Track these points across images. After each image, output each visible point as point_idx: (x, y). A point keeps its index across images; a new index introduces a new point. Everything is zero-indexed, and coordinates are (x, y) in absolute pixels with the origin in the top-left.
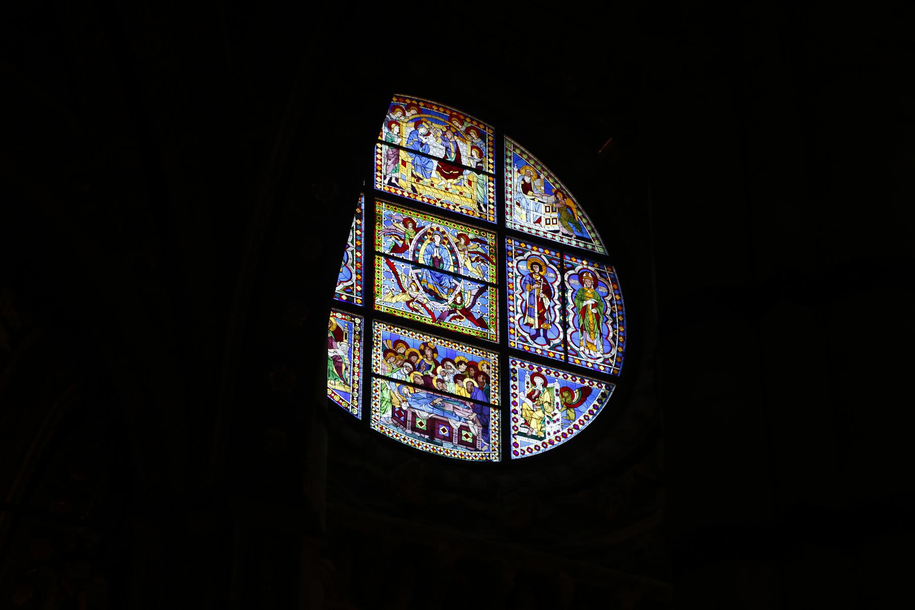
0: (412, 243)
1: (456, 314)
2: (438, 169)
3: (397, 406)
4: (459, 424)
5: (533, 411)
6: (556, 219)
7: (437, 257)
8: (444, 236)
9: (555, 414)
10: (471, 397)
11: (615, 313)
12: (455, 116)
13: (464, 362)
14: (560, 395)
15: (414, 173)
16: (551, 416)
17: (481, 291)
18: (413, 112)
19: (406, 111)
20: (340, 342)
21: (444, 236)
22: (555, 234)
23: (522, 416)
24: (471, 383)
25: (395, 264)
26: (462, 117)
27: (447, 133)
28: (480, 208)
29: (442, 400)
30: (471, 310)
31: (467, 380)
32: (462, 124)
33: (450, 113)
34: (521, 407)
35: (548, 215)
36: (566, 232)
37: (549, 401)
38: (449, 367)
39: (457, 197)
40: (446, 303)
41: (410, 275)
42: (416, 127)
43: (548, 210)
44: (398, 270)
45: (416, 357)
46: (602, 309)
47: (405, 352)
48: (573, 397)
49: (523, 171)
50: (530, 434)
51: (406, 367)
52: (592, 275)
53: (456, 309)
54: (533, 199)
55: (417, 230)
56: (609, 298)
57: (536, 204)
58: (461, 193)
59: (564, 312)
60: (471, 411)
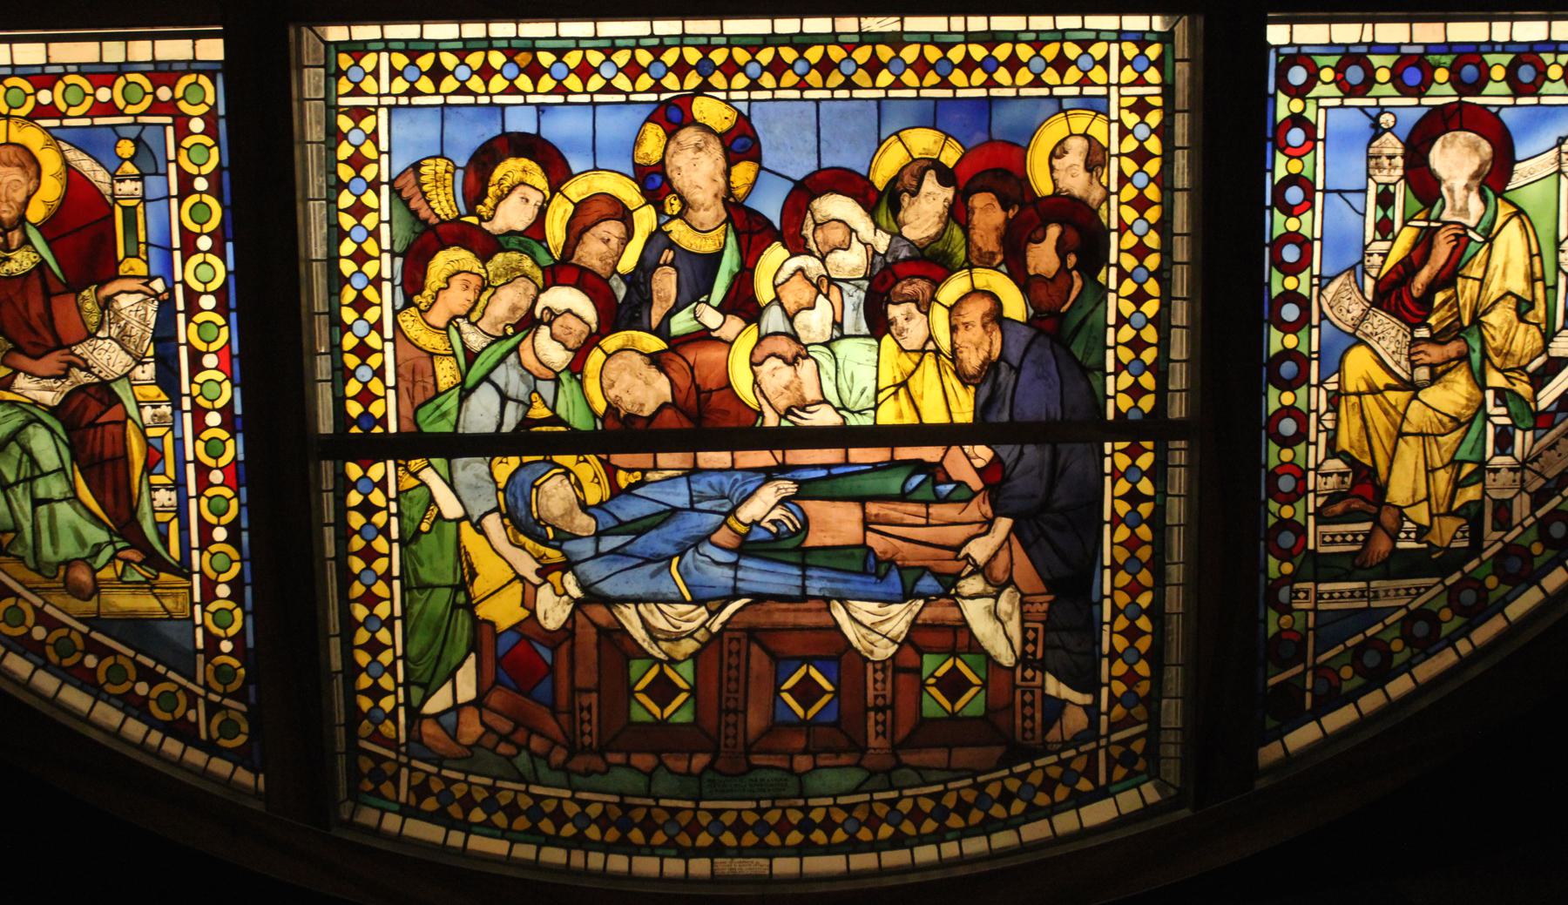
3: (503, 611)
4: (899, 618)
10: (981, 410)
13: (936, 165)
16: (1523, 389)
20: (102, 284)
23: (1332, 450)
24: (985, 305)
29: (789, 488)
37: (1518, 285)
38: (837, 235)
45: (613, 229)
47: (542, 212)
50: (1382, 545)
51: (553, 315)
60: (978, 509)
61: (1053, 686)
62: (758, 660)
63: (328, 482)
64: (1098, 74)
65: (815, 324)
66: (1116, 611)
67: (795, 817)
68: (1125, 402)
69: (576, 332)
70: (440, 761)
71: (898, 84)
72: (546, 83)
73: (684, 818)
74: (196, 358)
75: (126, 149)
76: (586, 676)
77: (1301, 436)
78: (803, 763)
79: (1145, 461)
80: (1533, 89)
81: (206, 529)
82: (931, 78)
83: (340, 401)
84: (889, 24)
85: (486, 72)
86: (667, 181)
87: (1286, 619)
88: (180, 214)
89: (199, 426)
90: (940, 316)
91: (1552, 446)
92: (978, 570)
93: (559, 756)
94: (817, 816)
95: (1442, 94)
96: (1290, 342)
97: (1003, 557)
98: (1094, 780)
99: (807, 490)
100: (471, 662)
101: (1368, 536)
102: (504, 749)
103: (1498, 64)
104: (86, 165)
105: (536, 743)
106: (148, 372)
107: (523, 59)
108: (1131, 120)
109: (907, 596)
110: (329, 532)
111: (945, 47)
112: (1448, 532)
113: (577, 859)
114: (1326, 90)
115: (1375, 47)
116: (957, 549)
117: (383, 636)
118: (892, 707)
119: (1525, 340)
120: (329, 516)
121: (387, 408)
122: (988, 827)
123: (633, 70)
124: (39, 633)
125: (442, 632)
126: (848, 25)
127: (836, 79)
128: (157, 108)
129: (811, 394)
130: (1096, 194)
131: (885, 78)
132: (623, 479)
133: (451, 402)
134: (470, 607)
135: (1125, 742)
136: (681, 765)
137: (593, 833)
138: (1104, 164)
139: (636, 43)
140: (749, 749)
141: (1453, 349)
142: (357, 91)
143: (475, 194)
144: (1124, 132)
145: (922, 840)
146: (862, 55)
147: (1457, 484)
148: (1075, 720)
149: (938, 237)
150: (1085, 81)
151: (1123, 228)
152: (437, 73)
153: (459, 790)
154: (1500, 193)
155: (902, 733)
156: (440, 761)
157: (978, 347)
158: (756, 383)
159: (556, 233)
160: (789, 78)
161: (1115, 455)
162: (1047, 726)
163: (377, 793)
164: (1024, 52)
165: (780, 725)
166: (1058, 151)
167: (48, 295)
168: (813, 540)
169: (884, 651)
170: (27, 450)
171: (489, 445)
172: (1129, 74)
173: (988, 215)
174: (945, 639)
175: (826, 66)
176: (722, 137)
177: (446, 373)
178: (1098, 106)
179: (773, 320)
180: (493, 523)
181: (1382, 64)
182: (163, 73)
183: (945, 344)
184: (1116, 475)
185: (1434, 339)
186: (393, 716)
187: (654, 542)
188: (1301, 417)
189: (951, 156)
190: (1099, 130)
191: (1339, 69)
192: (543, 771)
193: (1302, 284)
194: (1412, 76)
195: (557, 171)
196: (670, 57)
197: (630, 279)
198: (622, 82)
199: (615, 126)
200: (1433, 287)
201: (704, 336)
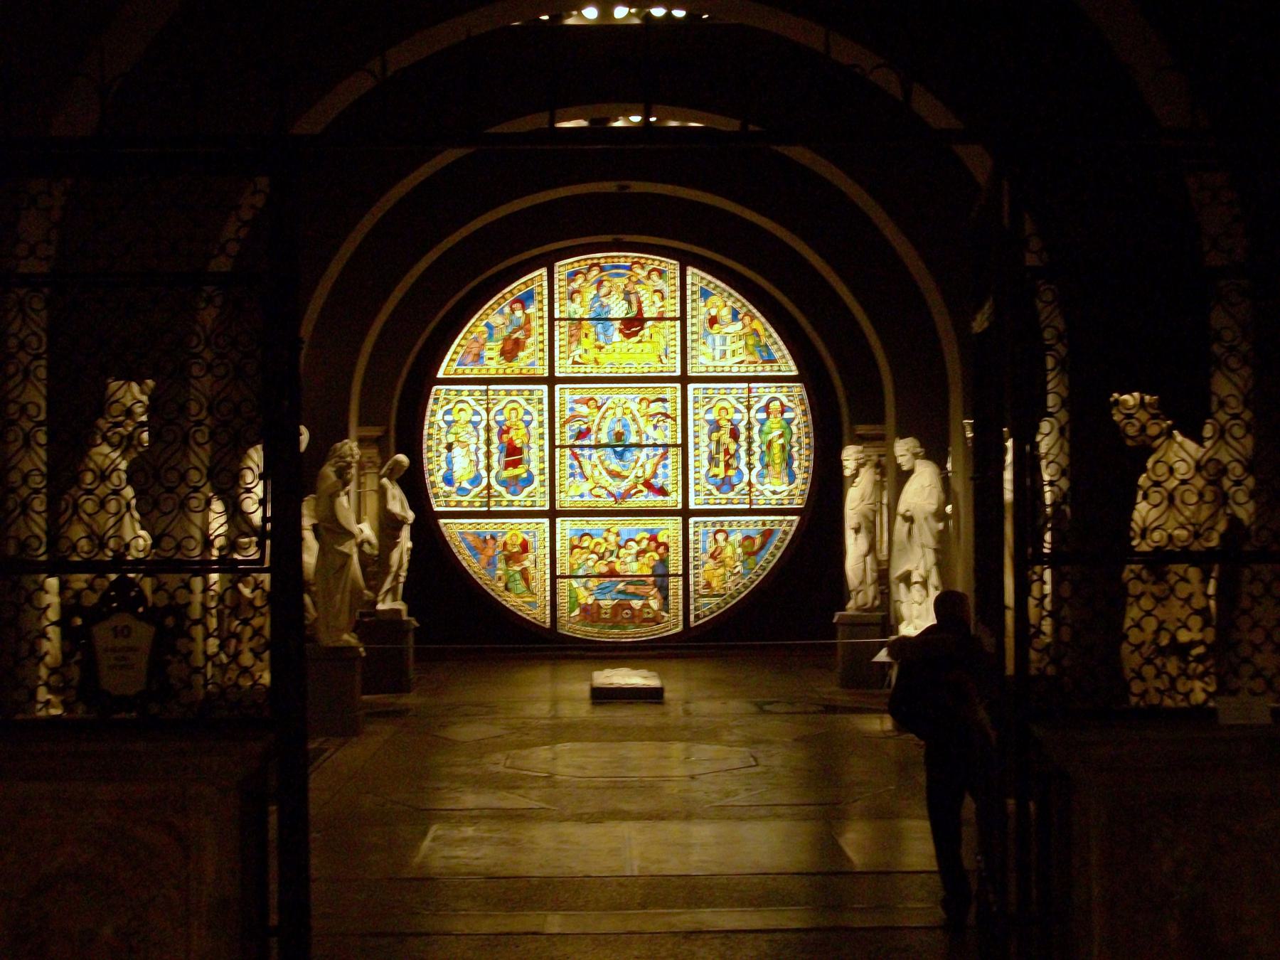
2: (621, 331)
3: (582, 601)
10: (653, 572)
17: (664, 457)
18: (595, 272)
26: (643, 261)
32: (643, 267)
35: (734, 347)
36: (751, 358)
42: (598, 288)
44: (581, 459)
46: (788, 437)
49: (709, 304)
59: (749, 452)
112: (722, 592)
148: (666, 619)
159: (592, 546)
173: (653, 544)
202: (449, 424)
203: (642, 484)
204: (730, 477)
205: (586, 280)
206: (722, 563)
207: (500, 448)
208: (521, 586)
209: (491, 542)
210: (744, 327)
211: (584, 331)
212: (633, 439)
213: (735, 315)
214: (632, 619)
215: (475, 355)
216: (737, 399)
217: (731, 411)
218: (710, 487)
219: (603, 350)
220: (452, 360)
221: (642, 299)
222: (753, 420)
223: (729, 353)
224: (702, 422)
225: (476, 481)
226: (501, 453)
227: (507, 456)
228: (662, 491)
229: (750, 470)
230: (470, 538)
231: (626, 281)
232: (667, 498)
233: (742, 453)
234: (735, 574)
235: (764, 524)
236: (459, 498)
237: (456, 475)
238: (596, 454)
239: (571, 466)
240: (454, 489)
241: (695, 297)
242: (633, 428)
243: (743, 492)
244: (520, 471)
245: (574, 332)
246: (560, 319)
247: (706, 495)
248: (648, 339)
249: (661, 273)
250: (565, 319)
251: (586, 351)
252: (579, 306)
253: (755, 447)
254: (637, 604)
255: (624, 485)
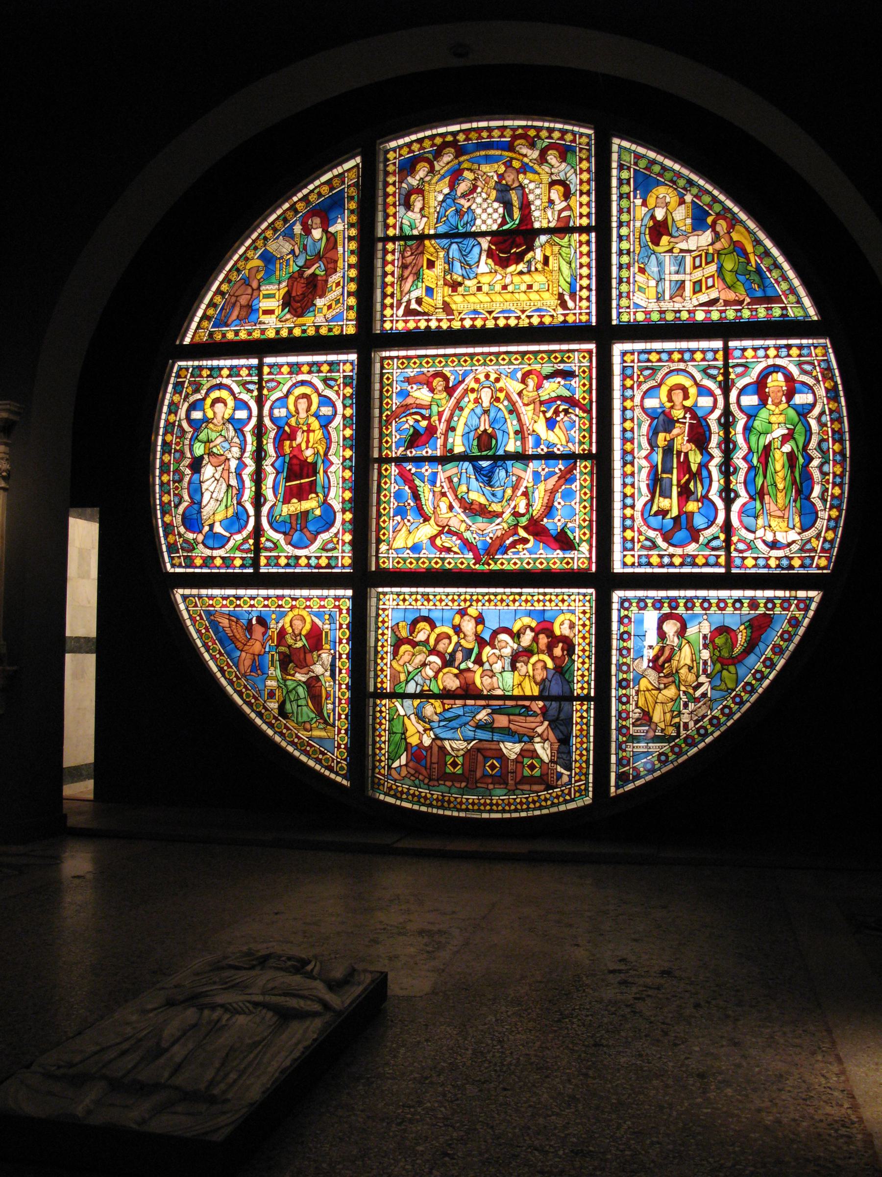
0: (443, 420)
1: (516, 538)
2: (490, 254)
3: (414, 740)
4: (518, 747)
5: (659, 689)
6: (713, 276)
7: (485, 430)
8: (498, 385)
9: (700, 685)
10: (541, 692)
11: (827, 440)
12: (521, 136)
13: (530, 627)
14: (711, 646)
15: (448, 277)
16: (691, 691)
17: (567, 477)
18: (448, 157)
19: (435, 163)
20: (318, 651)
21: (498, 385)
22: (711, 308)
23: (637, 706)
24: (541, 664)
25: (413, 470)
26: (532, 133)
27: (506, 175)
28: (563, 304)
29: (489, 711)
30: (545, 520)
31: (534, 659)
32: (532, 145)
33: (511, 133)
34: (636, 688)
35: (698, 275)
36: (731, 296)
37: (689, 662)
38: (503, 644)
39: (523, 297)
40: (500, 520)
41: (438, 484)
42: (452, 186)
43: (697, 264)
44: (417, 482)
45: (446, 641)
46: (801, 441)
48: (734, 645)
49: (651, 201)
50: (651, 734)
51: (430, 663)
52: (784, 374)
53: (516, 526)
54: (670, 251)
55: (450, 391)
56: (816, 411)
57: (676, 257)
58: (530, 287)
59: (727, 469)
61: (559, 769)
62: (480, 757)
63: (371, 704)
64: (572, 604)
65: (497, 667)
66: (577, 749)
67: (488, 801)
68: (579, 691)
69: (436, 667)
70: (395, 780)
71: (520, 605)
72: (431, 603)
73: (459, 800)
74: (340, 670)
75: (327, 617)
76: (435, 760)
77: (628, 702)
78: (491, 786)
79: (585, 707)
80: (692, 609)
81: (340, 715)
82: (529, 604)
83: (375, 683)
84: (518, 590)
85: (416, 600)
86: (460, 629)
87: (624, 754)
88: (339, 634)
89: (340, 688)
90: (530, 666)
91: (700, 707)
92: (539, 735)
93: (426, 781)
94: (494, 802)
95: (666, 610)
96: (625, 676)
97: (546, 732)
98: (570, 796)
99: (494, 712)
100: (405, 754)
101: (647, 732)
102: (412, 778)
103: (682, 602)
104: (316, 620)
105: (421, 777)
106: (328, 674)
107: (426, 597)
108: (581, 616)
109: (520, 742)
110: (371, 717)
111: (533, 596)
112: (672, 731)
113: (430, 810)
114: (634, 608)
115: (647, 597)
116: (534, 729)
117: (383, 746)
118: (515, 772)
119: (691, 677)
120: (371, 713)
121: (388, 686)
122: (541, 808)
123: (453, 601)
124: (296, 740)
125: (398, 746)
126: (508, 590)
127: (504, 604)
128: (335, 607)
129: (496, 686)
130: (572, 635)
131: (517, 604)
132: (447, 707)
133: (404, 685)
134: (405, 739)
135: (579, 786)
136: (458, 785)
137: (434, 803)
138: (574, 627)
139: (454, 594)
140: (476, 782)
141: (670, 679)
142: (384, 604)
143: (412, 631)
144: (580, 619)
145: (523, 810)
146: (511, 598)
147: (673, 717)
148: (565, 779)
149: (530, 646)
150: (569, 605)
151: (579, 644)
152: (404, 600)
153: (400, 789)
154: (683, 637)
155: (518, 780)
156: (395, 780)
157: (540, 675)
158: (482, 682)
159: (432, 642)
160: (493, 603)
161: (576, 705)
162: (557, 780)
163: (378, 789)
164: (553, 598)
165: (485, 776)
166: (562, 624)
167: (305, 653)
168: (495, 726)
169: (513, 756)
170: (297, 692)
171: (413, 696)
172: (581, 604)
173: (543, 640)
174: (530, 754)
175: (502, 601)
176: (475, 618)
177: (403, 677)
178: (573, 612)
179: (487, 666)
180: (412, 717)
181: (649, 602)
182: (337, 598)
183: (531, 674)
184: (577, 711)
185: (665, 677)
186: (384, 768)
187: (454, 724)
188: (628, 697)
189: (534, 624)
190: (573, 618)
191: (638, 603)
192: (422, 785)
193: (628, 660)
194: (658, 605)
195: (433, 626)
196: (462, 597)
197: (450, 654)
198: (450, 603)
199: (448, 615)
200: (664, 662)
201: (468, 670)
202: (197, 426)
203: (525, 528)
204: (690, 516)
205: (432, 170)
206: (673, 678)
207: (277, 465)
208: (307, 712)
209: (258, 630)
210: (717, 237)
211: (427, 256)
212: (512, 446)
213: (699, 221)
214: (501, 780)
215: (241, 306)
216: (704, 371)
217: (693, 391)
218: (652, 534)
219: (460, 289)
220: (205, 317)
221: (531, 197)
222: (734, 408)
223: (688, 286)
224: (638, 411)
225: (236, 521)
226: (278, 473)
227: (288, 479)
228: (564, 541)
229: (728, 503)
230: (225, 622)
231: (502, 169)
232: (569, 555)
233: (714, 467)
234: (696, 700)
235: (754, 604)
236: (208, 552)
237: (205, 512)
238: (443, 473)
239: (398, 495)
240: (200, 538)
241: (625, 189)
242: (512, 425)
243: (714, 543)
244: (310, 504)
245: (409, 260)
246: (387, 239)
247: (643, 547)
248: (539, 266)
249: (564, 152)
250: (394, 239)
251: (429, 291)
252: (419, 216)
253: (738, 459)
254: (511, 749)
255: (494, 529)
